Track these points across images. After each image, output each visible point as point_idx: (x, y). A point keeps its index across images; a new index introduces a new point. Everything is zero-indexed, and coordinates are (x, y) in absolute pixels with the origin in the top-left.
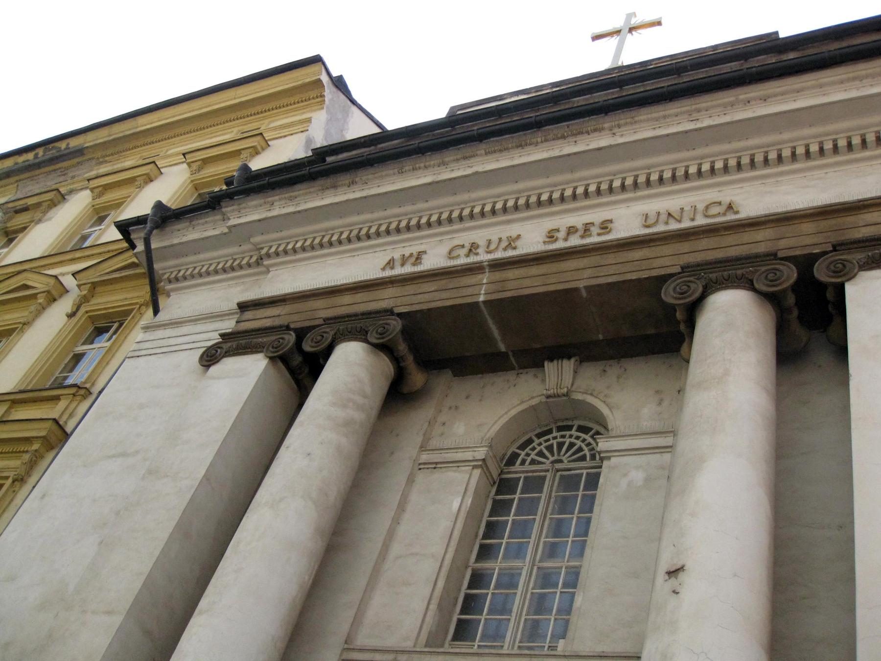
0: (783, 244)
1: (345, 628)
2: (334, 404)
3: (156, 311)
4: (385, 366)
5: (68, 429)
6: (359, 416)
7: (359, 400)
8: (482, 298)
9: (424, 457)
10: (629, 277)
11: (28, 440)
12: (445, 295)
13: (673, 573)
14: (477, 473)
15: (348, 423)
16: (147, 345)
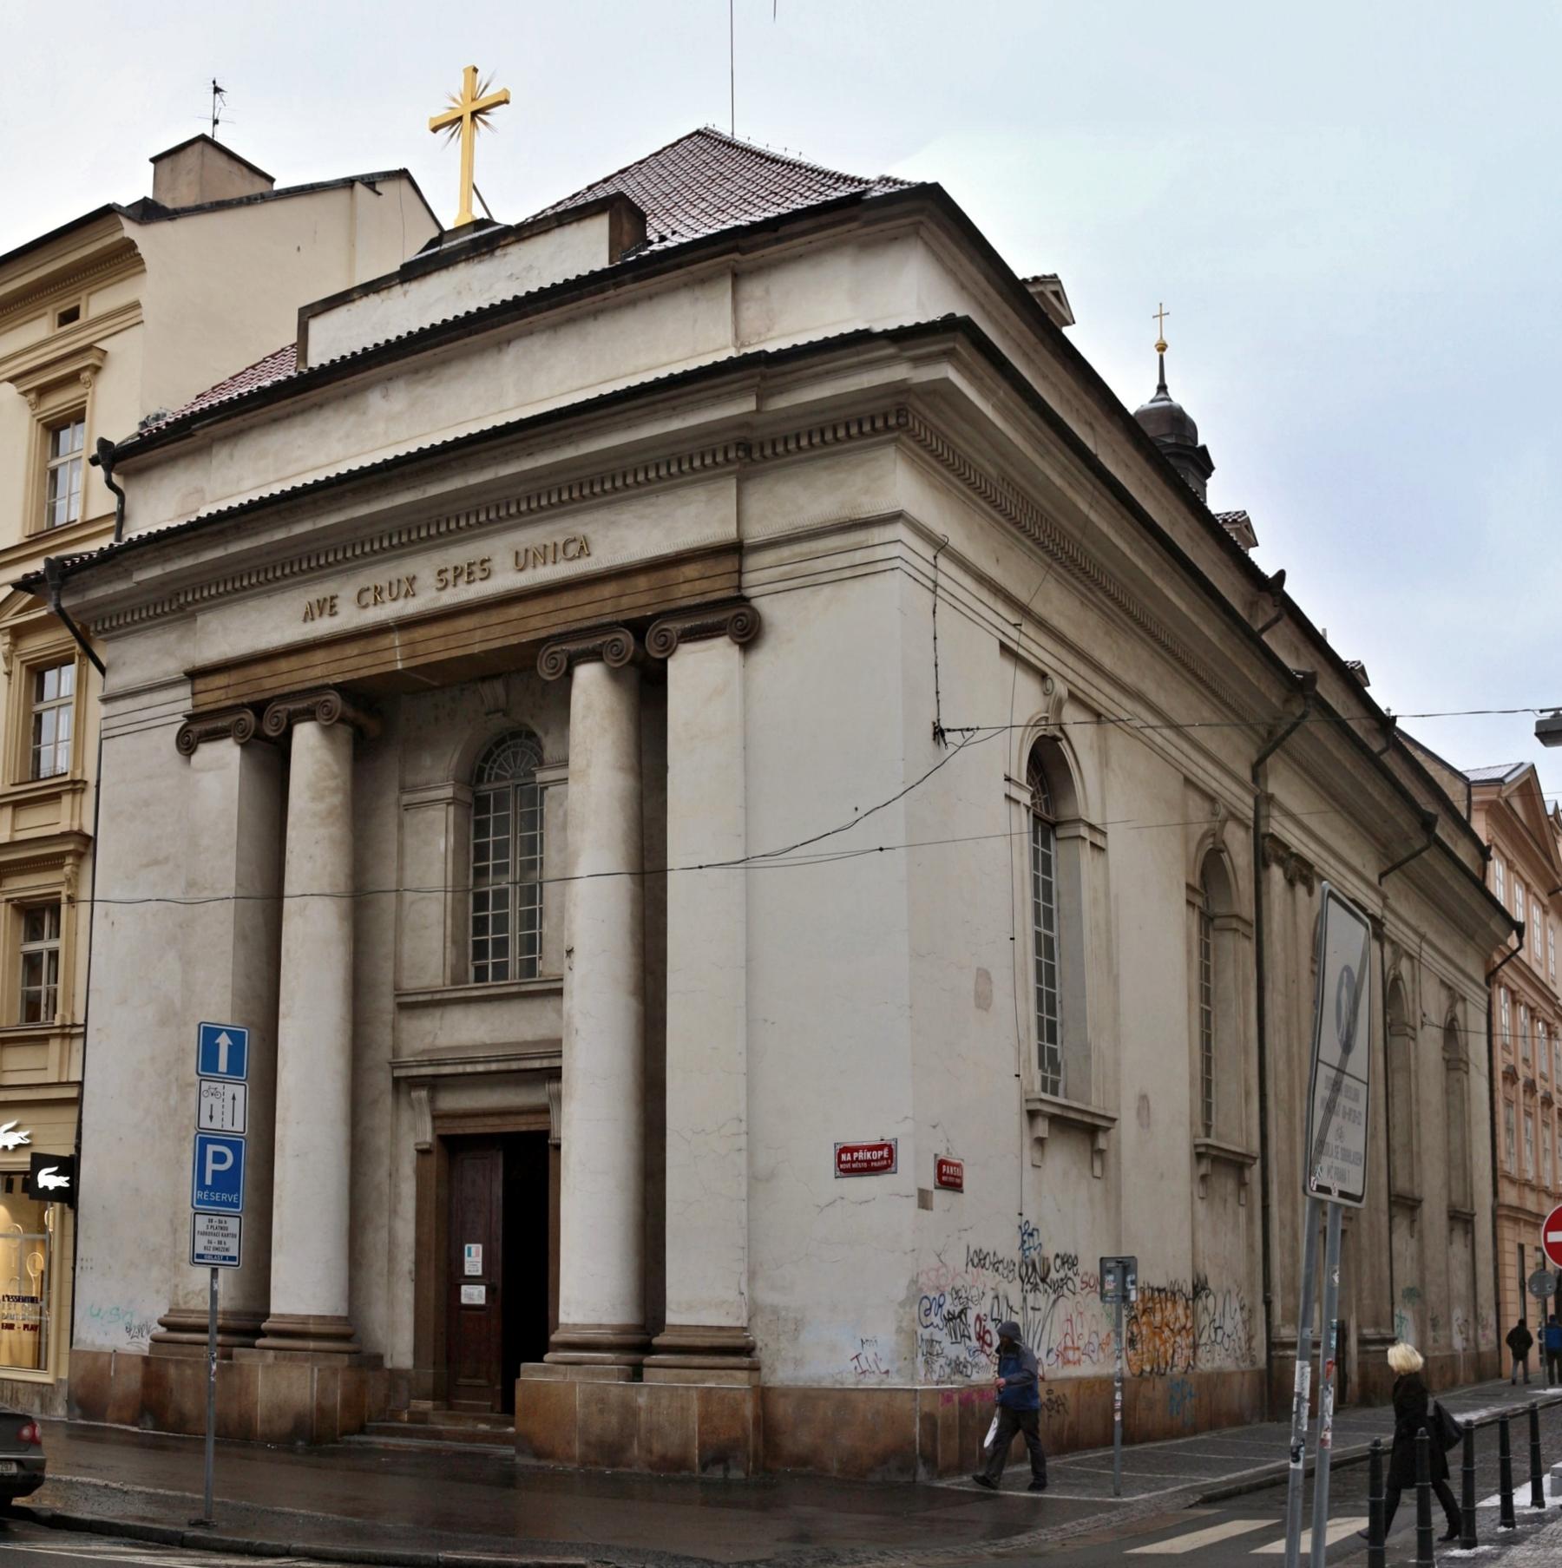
0: (625, 602)
1: (391, 976)
2: (313, 799)
4: (344, 732)
5: (90, 832)
6: (337, 800)
7: (332, 784)
8: (400, 666)
10: (514, 641)
12: (368, 661)
13: (570, 952)
14: (451, 808)
15: (330, 813)
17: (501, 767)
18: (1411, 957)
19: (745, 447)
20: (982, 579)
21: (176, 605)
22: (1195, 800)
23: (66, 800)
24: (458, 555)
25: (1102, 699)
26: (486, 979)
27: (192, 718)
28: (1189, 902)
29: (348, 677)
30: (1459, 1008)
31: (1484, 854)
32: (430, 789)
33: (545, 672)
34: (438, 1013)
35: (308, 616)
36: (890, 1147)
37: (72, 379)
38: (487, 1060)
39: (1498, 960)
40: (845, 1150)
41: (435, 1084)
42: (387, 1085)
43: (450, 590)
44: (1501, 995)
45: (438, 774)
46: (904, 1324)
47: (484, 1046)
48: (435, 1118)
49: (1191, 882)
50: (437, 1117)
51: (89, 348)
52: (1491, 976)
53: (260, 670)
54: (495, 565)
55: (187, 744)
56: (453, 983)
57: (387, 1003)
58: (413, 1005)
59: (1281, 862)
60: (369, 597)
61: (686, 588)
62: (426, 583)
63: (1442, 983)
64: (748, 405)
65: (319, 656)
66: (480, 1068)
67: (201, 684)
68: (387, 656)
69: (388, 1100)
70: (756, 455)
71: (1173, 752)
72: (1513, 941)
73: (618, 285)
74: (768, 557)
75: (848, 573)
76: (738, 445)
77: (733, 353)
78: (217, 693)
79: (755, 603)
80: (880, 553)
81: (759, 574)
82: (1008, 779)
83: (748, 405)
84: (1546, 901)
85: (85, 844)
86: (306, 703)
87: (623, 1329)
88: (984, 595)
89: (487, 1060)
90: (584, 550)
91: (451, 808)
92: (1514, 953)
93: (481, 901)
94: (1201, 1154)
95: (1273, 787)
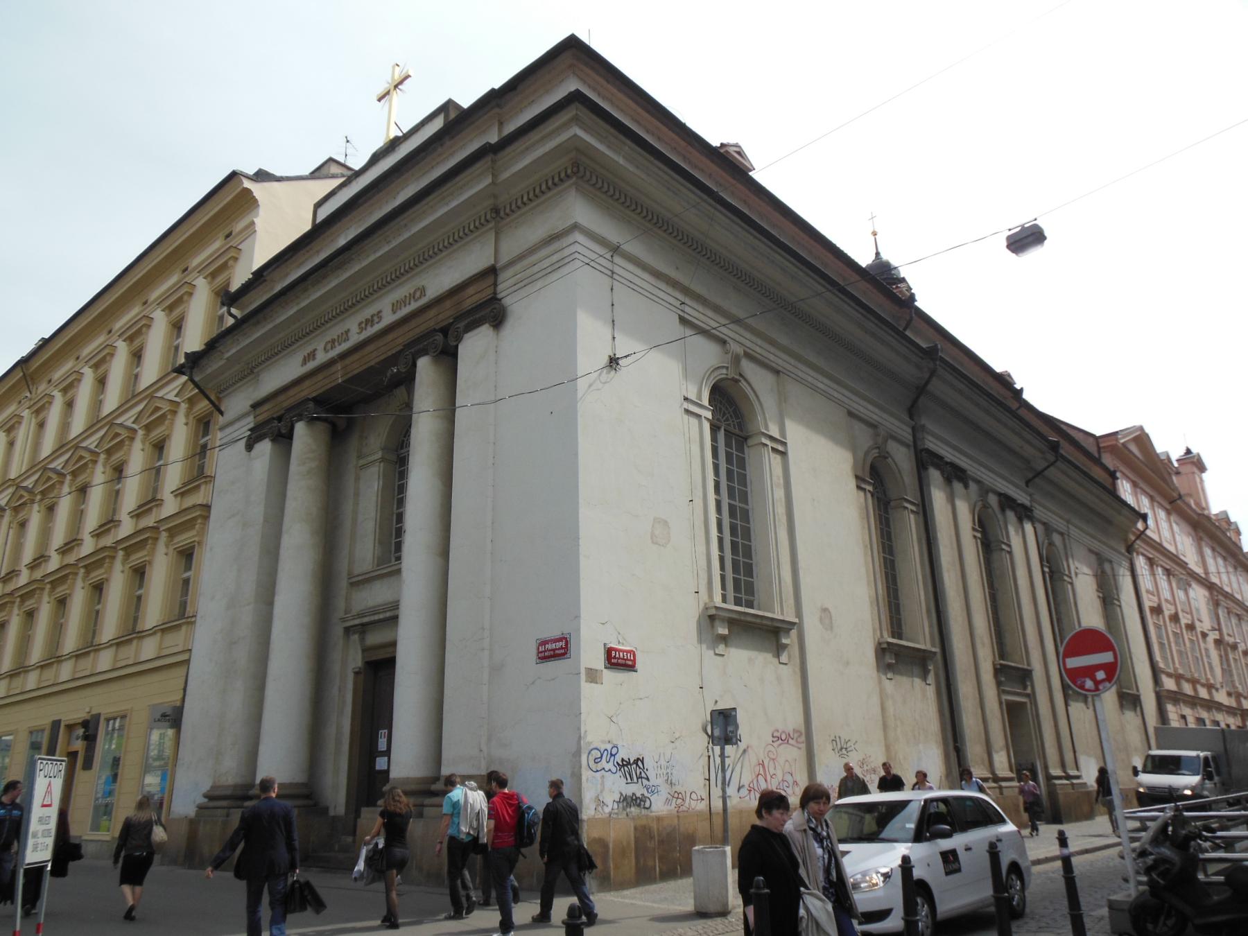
0: (441, 317)
9: (362, 462)
10: (389, 354)
18: (1062, 534)
20: (657, 275)
21: (250, 372)
22: (858, 427)
24: (368, 312)
25: (780, 362)
28: (859, 487)
30: (1107, 566)
31: (1113, 475)
35: (304, 362)
39: (1133, 538)
40: (544, 643)
41: (363, 629)
44: (1141, 562)
48: (364, 651)
49: (860, 474)
50: (365, 650)
52: (1130, 549)
54: (383, 314)
55: (249, 447)
58: (360, 582)
59: (937, 467)
63: (1091, 551)
65: (307, 383)
67: (258, 411)
70: (502, 213)
71: (836, 394)
72: (1140, 525)
74: (510, 272)
78: (265, 412)
82: (686, 399)
84: (1168, 507)
86: (296, 412)
88: (663, 286)
90: (423, 291)
92: (1143, 532)
94: (882, 650)
95: (924, 421)
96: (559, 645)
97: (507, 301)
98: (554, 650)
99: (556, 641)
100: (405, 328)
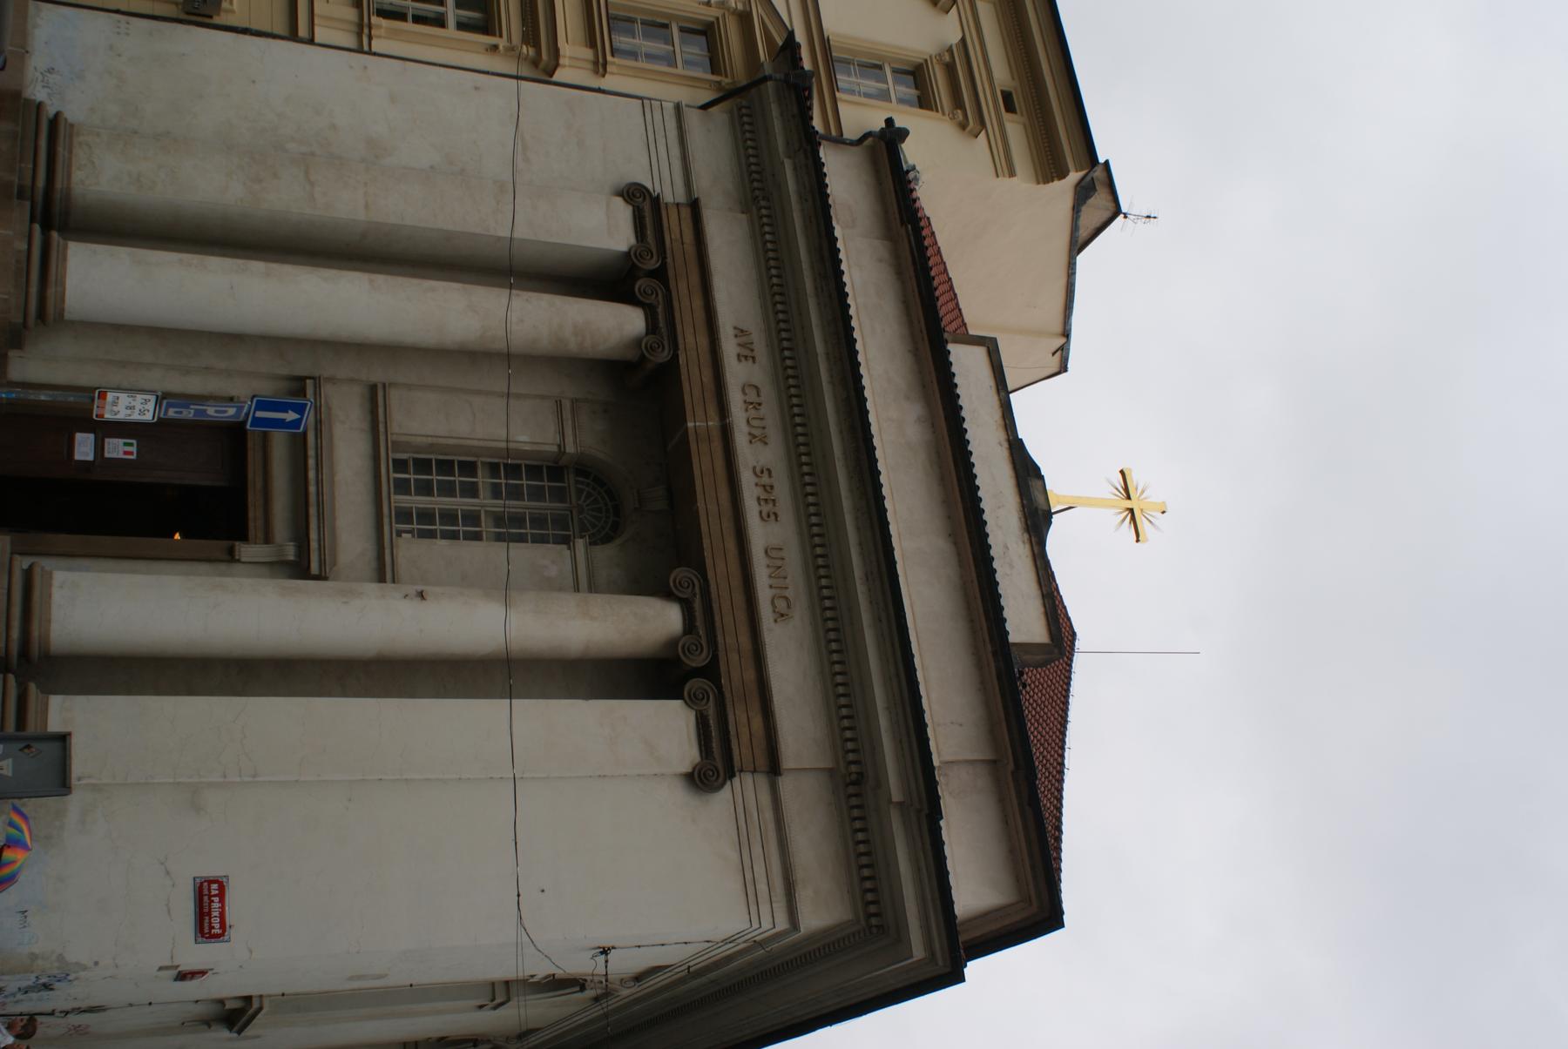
0: (734, 657)
3: (705, 107)
4: (631, 355)
5: (557, 77)
8: (690, 425)
10: (706, 543)
11: (537, 46)
12: (697, 392)
14: (555, 449)
16: (658, 116)
17: (589, 495)
19: (859, 780)
21: (755, 193)
23: (588, 54)
26: (395, 471)
27: (656, 201)
29: (683, 371)
32: (574, 428)
33: (680, 573)
34: (366, 425)
35: (740, 332)
36: (222, 935)
37: (958, 103)
38: (319, 482)
40: (222, 888)
42: (300, 371)
43: (754, 479)
45: (586, 438)
46: (40, 962)
47: (332, 475)
51: (983, 124)
53: (695, 278)
55: (632, 193)
56: (394, 443)
57: (377, 376)
58: (374, 398)
60: (752, 397)
61: (743, 719)
62: (759, 455)
64: (896, 796)
65: (703, 341)
66: (312, 475)
67: (686, 213)
68: (699, 412)
69: (285, 371)
70: (851, 790)
73: (995, 654)
74: (765, 799)
75: (749, 876)
76: (861, 774)
77: (936, 763)
78: (677, 228)
79: (728, 786)
80: (765, 909)
81: (749, 788)
83: (896, 796)
85: (544, 69)
87: (45, 638)
89: (319, 482)
90: (781, 616)
91: (555, 449)
93: (469, 468)
96: (216, 922)
97: (725, 793)
98: (209, 914)
99: (222, 916)
100: (736, 582)
